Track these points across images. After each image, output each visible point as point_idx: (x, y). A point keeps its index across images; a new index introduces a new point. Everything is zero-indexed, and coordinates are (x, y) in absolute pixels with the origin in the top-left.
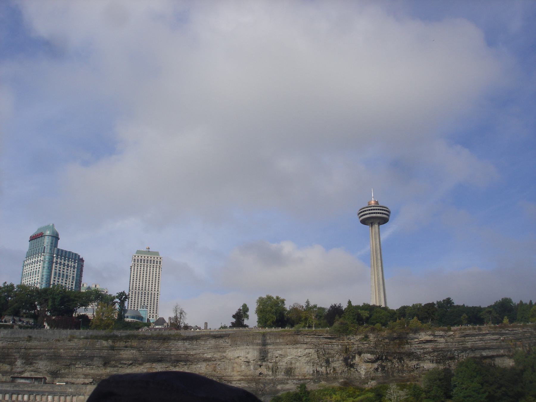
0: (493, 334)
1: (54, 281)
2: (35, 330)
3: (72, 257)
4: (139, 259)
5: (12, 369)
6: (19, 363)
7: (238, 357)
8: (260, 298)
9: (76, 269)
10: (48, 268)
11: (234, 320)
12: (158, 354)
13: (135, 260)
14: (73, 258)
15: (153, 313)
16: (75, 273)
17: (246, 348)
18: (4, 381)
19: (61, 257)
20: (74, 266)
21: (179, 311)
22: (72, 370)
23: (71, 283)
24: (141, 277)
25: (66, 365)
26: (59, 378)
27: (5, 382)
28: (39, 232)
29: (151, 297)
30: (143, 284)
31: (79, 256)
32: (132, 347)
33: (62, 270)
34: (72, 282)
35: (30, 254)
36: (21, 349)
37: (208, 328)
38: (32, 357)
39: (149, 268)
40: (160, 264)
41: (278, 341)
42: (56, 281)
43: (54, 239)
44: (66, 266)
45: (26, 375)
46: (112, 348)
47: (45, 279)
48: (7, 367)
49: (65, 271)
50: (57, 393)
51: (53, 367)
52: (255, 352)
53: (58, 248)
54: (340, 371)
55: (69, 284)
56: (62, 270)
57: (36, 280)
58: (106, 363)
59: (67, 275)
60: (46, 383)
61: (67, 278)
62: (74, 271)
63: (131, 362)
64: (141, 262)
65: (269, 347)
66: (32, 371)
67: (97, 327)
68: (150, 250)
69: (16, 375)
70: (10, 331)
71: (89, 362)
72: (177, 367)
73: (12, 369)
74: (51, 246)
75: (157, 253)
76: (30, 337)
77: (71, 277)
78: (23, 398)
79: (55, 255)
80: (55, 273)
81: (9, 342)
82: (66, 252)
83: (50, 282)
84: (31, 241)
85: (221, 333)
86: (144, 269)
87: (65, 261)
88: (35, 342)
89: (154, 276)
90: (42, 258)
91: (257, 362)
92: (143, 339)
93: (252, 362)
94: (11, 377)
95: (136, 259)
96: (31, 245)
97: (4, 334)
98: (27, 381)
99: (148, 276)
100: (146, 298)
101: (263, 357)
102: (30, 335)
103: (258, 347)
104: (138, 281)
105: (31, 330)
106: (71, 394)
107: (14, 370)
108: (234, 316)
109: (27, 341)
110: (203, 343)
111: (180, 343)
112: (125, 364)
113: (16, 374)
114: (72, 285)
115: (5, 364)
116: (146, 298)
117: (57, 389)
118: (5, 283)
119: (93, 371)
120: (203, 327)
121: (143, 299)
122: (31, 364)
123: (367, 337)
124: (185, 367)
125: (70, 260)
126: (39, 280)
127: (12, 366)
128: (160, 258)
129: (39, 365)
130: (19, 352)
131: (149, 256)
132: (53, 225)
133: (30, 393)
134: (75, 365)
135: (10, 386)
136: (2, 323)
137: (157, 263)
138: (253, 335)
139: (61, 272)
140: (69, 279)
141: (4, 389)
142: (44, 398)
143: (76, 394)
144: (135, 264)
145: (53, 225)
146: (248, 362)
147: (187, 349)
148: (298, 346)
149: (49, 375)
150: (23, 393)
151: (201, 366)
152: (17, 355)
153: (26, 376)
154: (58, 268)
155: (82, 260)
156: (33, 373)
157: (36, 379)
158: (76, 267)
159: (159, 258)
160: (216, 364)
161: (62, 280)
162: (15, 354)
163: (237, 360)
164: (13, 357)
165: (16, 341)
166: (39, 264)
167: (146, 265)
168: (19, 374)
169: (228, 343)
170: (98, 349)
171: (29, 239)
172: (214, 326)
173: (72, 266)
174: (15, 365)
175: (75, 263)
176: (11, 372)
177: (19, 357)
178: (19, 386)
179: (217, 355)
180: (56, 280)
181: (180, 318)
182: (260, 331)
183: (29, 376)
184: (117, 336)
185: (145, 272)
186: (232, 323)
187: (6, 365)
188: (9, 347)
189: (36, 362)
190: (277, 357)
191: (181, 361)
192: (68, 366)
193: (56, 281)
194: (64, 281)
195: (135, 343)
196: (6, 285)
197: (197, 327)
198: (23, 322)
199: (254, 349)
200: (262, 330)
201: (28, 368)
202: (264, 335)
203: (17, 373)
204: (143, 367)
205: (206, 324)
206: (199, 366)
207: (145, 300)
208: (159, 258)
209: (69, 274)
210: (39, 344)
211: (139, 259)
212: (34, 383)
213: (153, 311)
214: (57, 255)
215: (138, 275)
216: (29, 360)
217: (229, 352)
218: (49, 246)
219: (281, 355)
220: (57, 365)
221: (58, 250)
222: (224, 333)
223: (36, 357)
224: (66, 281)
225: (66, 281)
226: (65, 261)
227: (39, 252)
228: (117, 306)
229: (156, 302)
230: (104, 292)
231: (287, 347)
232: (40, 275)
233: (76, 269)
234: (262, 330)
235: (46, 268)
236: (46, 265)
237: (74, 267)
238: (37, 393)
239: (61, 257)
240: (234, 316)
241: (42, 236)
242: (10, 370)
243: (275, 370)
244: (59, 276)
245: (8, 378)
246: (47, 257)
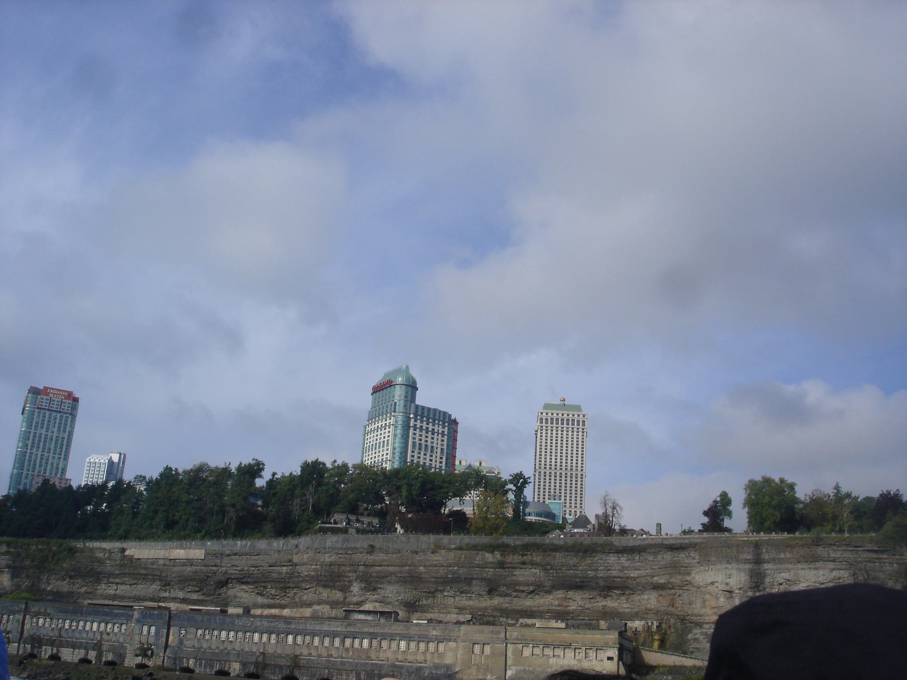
1: (413, 456)
2: (380, 535)
3: (439, 417)
4: (549, 418)
5: (345, 598)
6: (356, 588)
7: (712, 583)
8: (750, 481)
9: (446, 437)
10: (402, 436)
11: (706, 520)
12: (576, 576)
13: (541, 419)
14: (441, 419)
15: (576, 507)
16: (445, 443)
17: (726, 568)
18: (334, 616)
19: (422, 417)
20: (443, 432)
21: (610, 505)
22: (439, 601)
24: (554, 448)
25: (429, 593)
26: (418, 613)
27: (336, 618)
28: (387, 379)
29: (545, 479)
30: (556, 459)
31: (450, 416)
32: (533, 564)
33: (423, 438)
34: (441, 458)
35: (374, 416)
36: (358, 565)
37: (663, 533)
38: (376, 579)
39: (565, 433)
40: (584, 425)
41: (782, 555)
42: (416, 457)
43: (410, 389)
44: (430, 433)
45: (368, 607)
46: (501, 565)
47: (397, 455)
48: (338, 595)
49: (429, 440)
50: (415, 637)
51: (407, 594)
52: (743, 574)
53: (416, 403)
54: (176, 590)
56: (423, 438)
57: (384, 457)
58: (492, 591)
59: (432, 447)
60: (398, 621)
61: (432, 451)
62: (443, 441)
63: (531, 588)
64: (552, 423)
65: (766, 566)
66: (376, 601)
67: (478, 531)
68: (566, 403)
69: (352, 607)
70: (341, 537)
71: (464, 588)
72: (609, 598)
73: (345, 598)
74: (406, 401)
75: (578, 408)
76: (372, 547)
77: (439, 451)
78: (261, 639)
79: (412, 416)
80: (414, 443)
81: (339, 555)
82: (429, 409)
83: (406, 459)
84: (374, 394)
85: (682, 541)
86: (557, 434)
87: (428, 424)
88: (380, 554)
89: (575, 446)
90: (391, 421)
91: (746, 592)
92: (550, 550)
93: (736, 591)
94: (344, 610)
95: (544, 418)
96: (374, 400)
97: (331, 542)
98: (369, 618)
99: (564, 445)
100: (563, 482)
102: (372, 543)
103: (747, 566)
104: (548, 454)
105: (373, 535)
106: (436, 639)
107: (348, 600)
108: (706, 513)
109: (367, 553)
110: (651, 558)
111: (612, 559)
112: (523, 591)
113: (352, 606)
114: (441, 462)
115: (335, 590)
116: (563, 482)
117: (413, 631)
118: (335, 461)
119: (471, 603)
120: (653, 531)
121: (558, 485)
122: (375, 589)
124: (623, 598)
126: (388, 456)
127: (346, 592)
128: (584, 416)
129: (387, 592)
130: (355, 571)
131: (566, 412)
132: (407, 367)
133: (372, 636)
134: (442, 591)
135: (342, 624)
136: (330, 525)
137: (578, 425)
138: (738, 546)
139: (423, 442)
140: (435, 453)
141: (332, 629)
142: (394, 645)
143: (444, 639)
144: (542, 427)
145: (407, 367)
146: (730, 592)
147: (624, 568)
148: (818, 564)
149: (403, 608)
150: (361, 635)
151: (650, 597)
152: (353, 576)
153: (367, 609)
154: (417, 437)
155: (455, 422)
156: (377, 604)
157: (382, 613)
158: (446, 433)
159: (581, 416)
160: (675, 594)
161: (425, 454)
162: (350, 574)
163: (710, 588)
164: (347, 579)
165: (351, 553)
166: (387, 430)
167: (560, 428)
168: (356, 606)
169: (694, 559)
170: (479, 566)
171: (371, 392)
172: (672, 530)
173: (440, 432)
174: (349, 591)
175: (444, 427)
176: (344, 603)
177: (356, 580)
178: (355, 625)
179: (676, 580)
180: (416, 454)
181: (613, 516)
182: (750, 539)
183: (371, 609)
184: (508, 546)
185: (559, 439)
186: (702, 524)
187: (336, 592)
188: (340, 563)
189: (382, 586)
190: (781, 584)
191: (616, 588)
192: (432, 594)
193: (416, 457)
194: (428, 457)
195: (537, 558)
196: (336, 464)
197: (643, 531)
198: (363, 523)
199: (740, 570)
200: (754, 537)
201: (370, 596)
202: (757, 545)
203: (354, 604)
204: (551, 597)
205: (659, 525)
206: (646, 597)
207: (560, 486)
208: (581, 416)
209: (435, 445)
210: (385, 558)
211: (549, 418)
212: (379, 621)
213: (576, 504)
214: (416, 416)
215: (549, 444)
217: (696, 573)
218: (402, 402)
219: (788, 580)
220: (414, 592)
221: (417, 406)
222: (687, 541)
223: (383, 578)
224: (431, 456)
225: (431, 456)
226: (428, 424)
227: (387, 411)
228: (511, 496)
229: (579, 489)
230: (494, 473)
231: (799, 566)
232: (389, 447)
233: (446, 437)
234: (754, 537)
235: (399, 436)
236: (399, 432)
237: (443, 434)
238: (383, 636)
239: (422, 417)
240: (706, 513)
241: (390, 386)
242: (342, 600)
245: (340, 612)
246: (400, 419)
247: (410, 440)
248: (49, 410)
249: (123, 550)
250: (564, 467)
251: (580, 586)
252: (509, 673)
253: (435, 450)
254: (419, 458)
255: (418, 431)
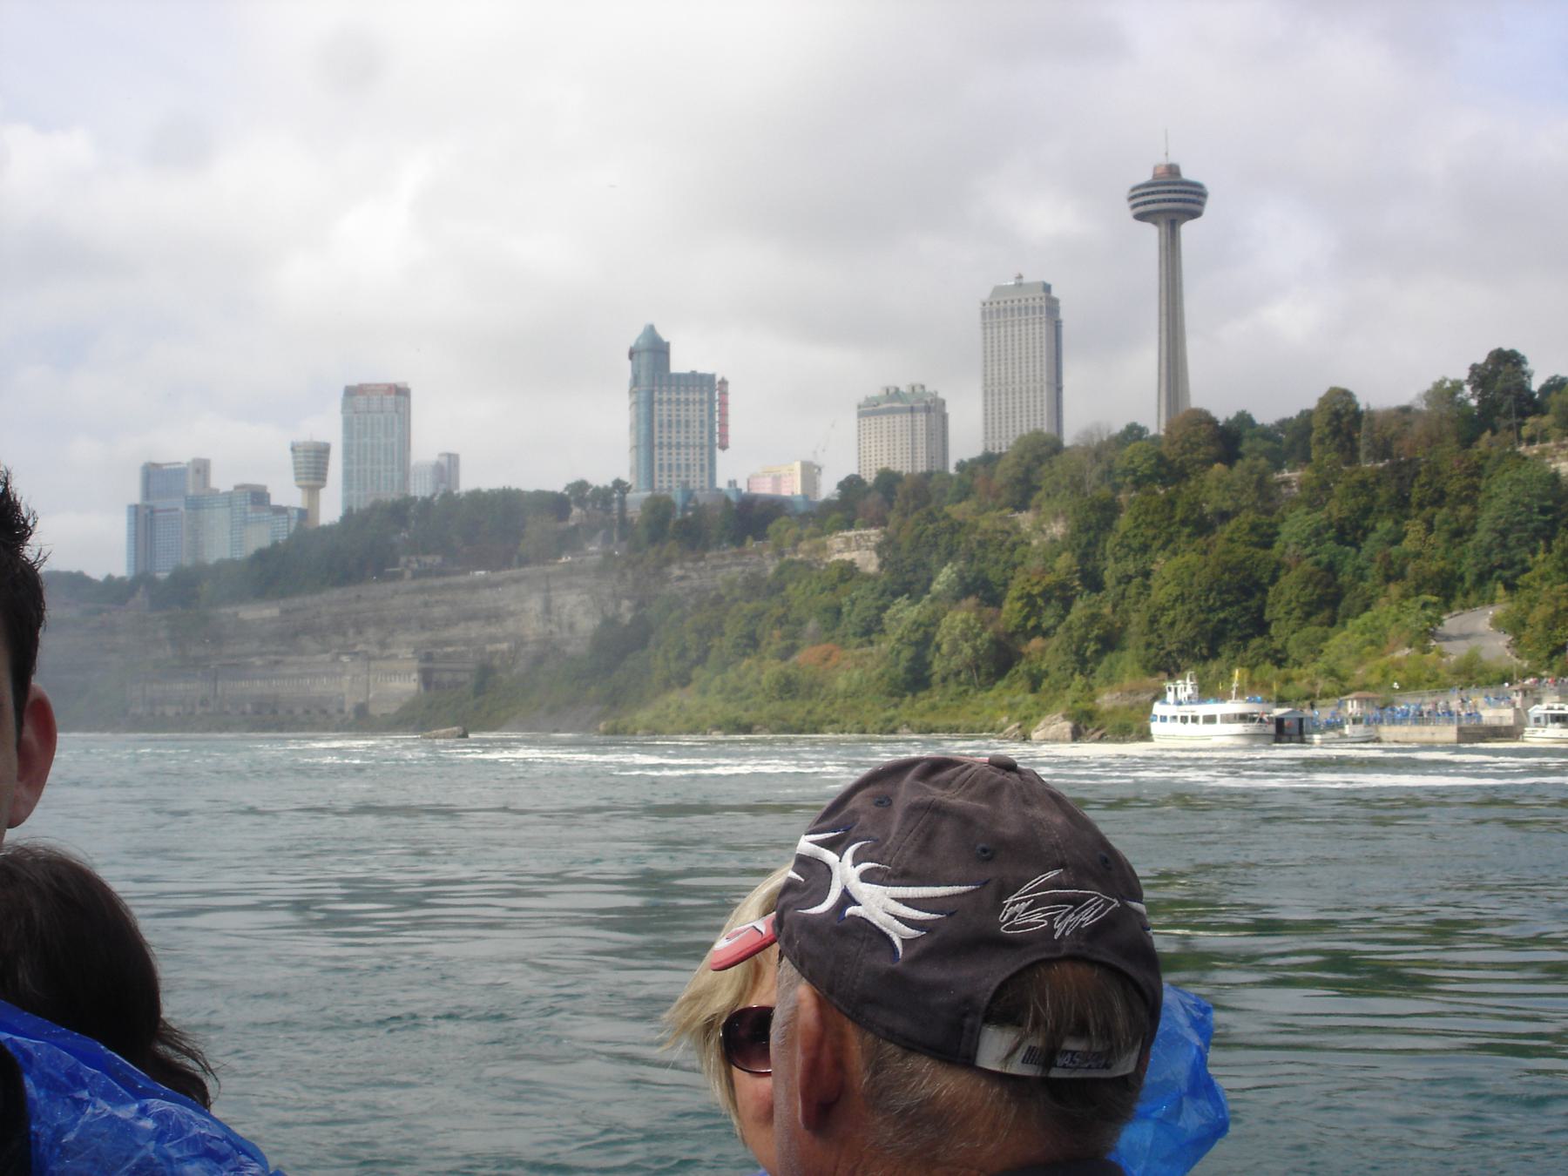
0: (738, 564)
6: (351, 632)
16: (706, 413)
23: (698, 435)
34: (701, 432)
46: (426, 604)
49: (683, 413)
55: (694, 437)
56: (674, 413)
58: (423, 627)
59: (687, 421)
68: (1026, 280)
76: (359, 596)
77: (697, 424)
87: (678, 393)
100: (1017, 400)
101: (547, 610)
111: (487, 593)
114: (701, 438)
123: (624, 574)
125: (691, 388)
137: (1034, 313)
139: (674, 418)
154: (665, 413)
161: (678, 432)
175: (701, 392)
180: (665, 435)
194: (683, 434)
216: (359, 628)
224: (687, 432)
225: (687, 432)
226: (678, 393)
228: (616, 506)
236: (643, 410)
237: (701, 402)
243: (560, 625)
244: (670, 426)
247: (656, 419)
248: (369, 412)
249: (236, 614)
250: (1017, 380)
251: (472, 617)
252: (371, 696)
253: (692, 424)
254: (670, 438)
255: (665, 407)
